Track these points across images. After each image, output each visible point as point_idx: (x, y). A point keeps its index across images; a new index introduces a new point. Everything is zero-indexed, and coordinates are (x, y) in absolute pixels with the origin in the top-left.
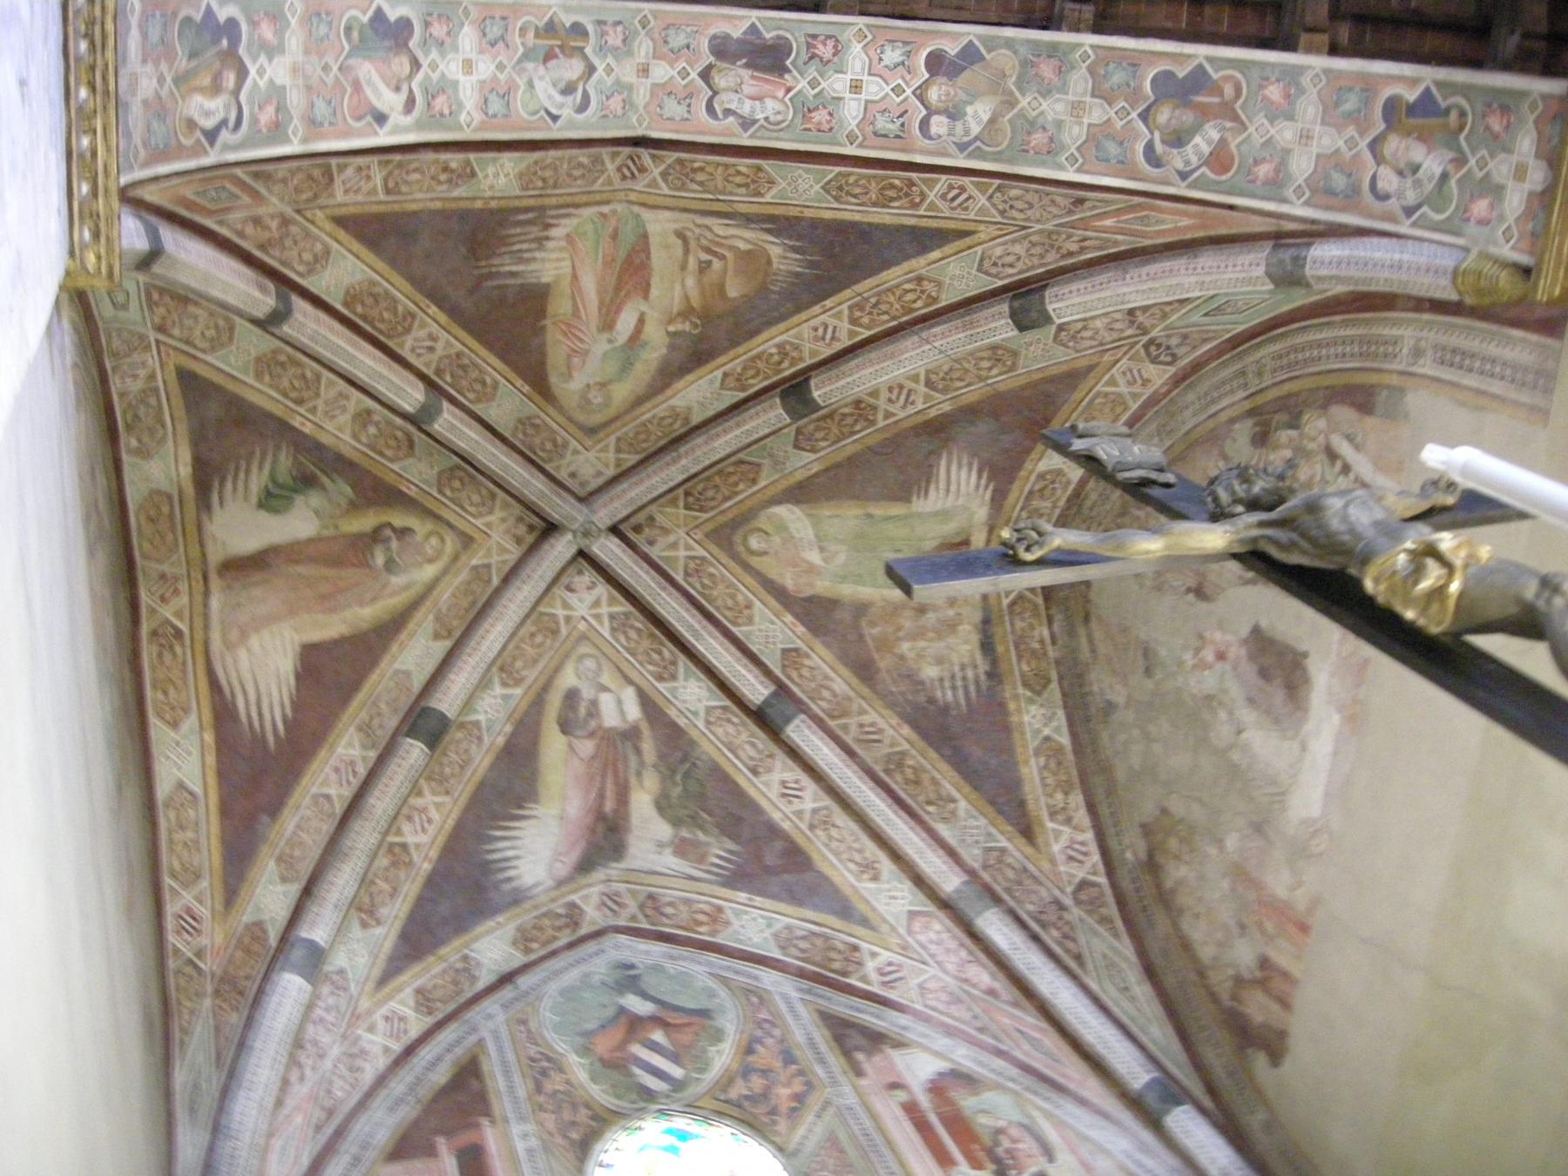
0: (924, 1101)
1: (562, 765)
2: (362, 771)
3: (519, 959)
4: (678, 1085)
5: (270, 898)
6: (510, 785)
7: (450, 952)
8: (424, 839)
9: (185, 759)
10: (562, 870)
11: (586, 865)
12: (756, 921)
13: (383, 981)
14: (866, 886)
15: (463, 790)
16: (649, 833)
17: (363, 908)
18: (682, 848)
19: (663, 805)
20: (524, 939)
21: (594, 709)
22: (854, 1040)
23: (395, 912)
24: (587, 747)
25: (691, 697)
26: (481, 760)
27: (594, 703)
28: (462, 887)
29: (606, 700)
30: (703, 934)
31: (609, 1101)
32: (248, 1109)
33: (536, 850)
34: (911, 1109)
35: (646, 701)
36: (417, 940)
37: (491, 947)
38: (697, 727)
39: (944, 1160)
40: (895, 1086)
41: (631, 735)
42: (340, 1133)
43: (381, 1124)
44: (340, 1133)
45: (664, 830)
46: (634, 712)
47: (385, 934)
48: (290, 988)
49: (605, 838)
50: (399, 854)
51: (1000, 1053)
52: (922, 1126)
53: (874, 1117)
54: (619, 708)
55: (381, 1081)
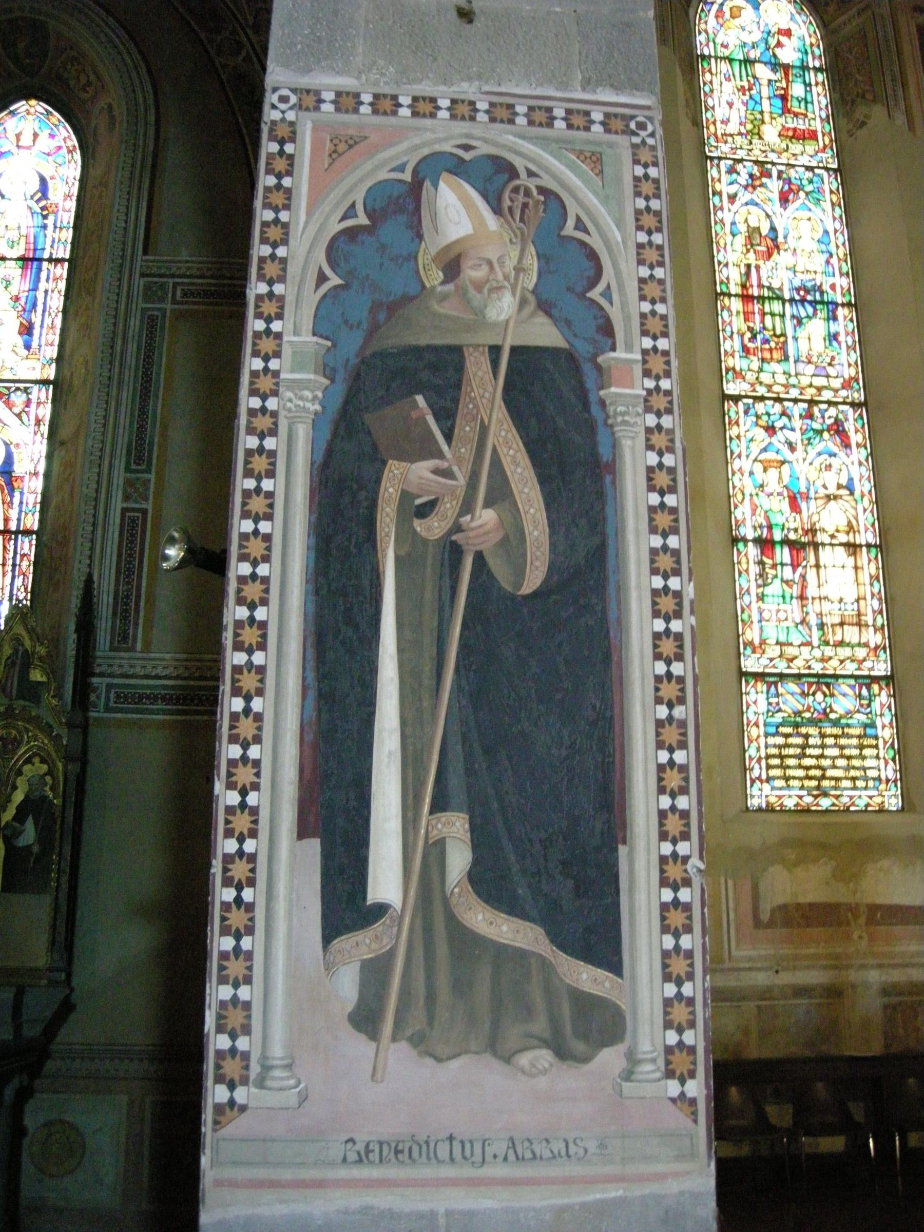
53: (896, 31)
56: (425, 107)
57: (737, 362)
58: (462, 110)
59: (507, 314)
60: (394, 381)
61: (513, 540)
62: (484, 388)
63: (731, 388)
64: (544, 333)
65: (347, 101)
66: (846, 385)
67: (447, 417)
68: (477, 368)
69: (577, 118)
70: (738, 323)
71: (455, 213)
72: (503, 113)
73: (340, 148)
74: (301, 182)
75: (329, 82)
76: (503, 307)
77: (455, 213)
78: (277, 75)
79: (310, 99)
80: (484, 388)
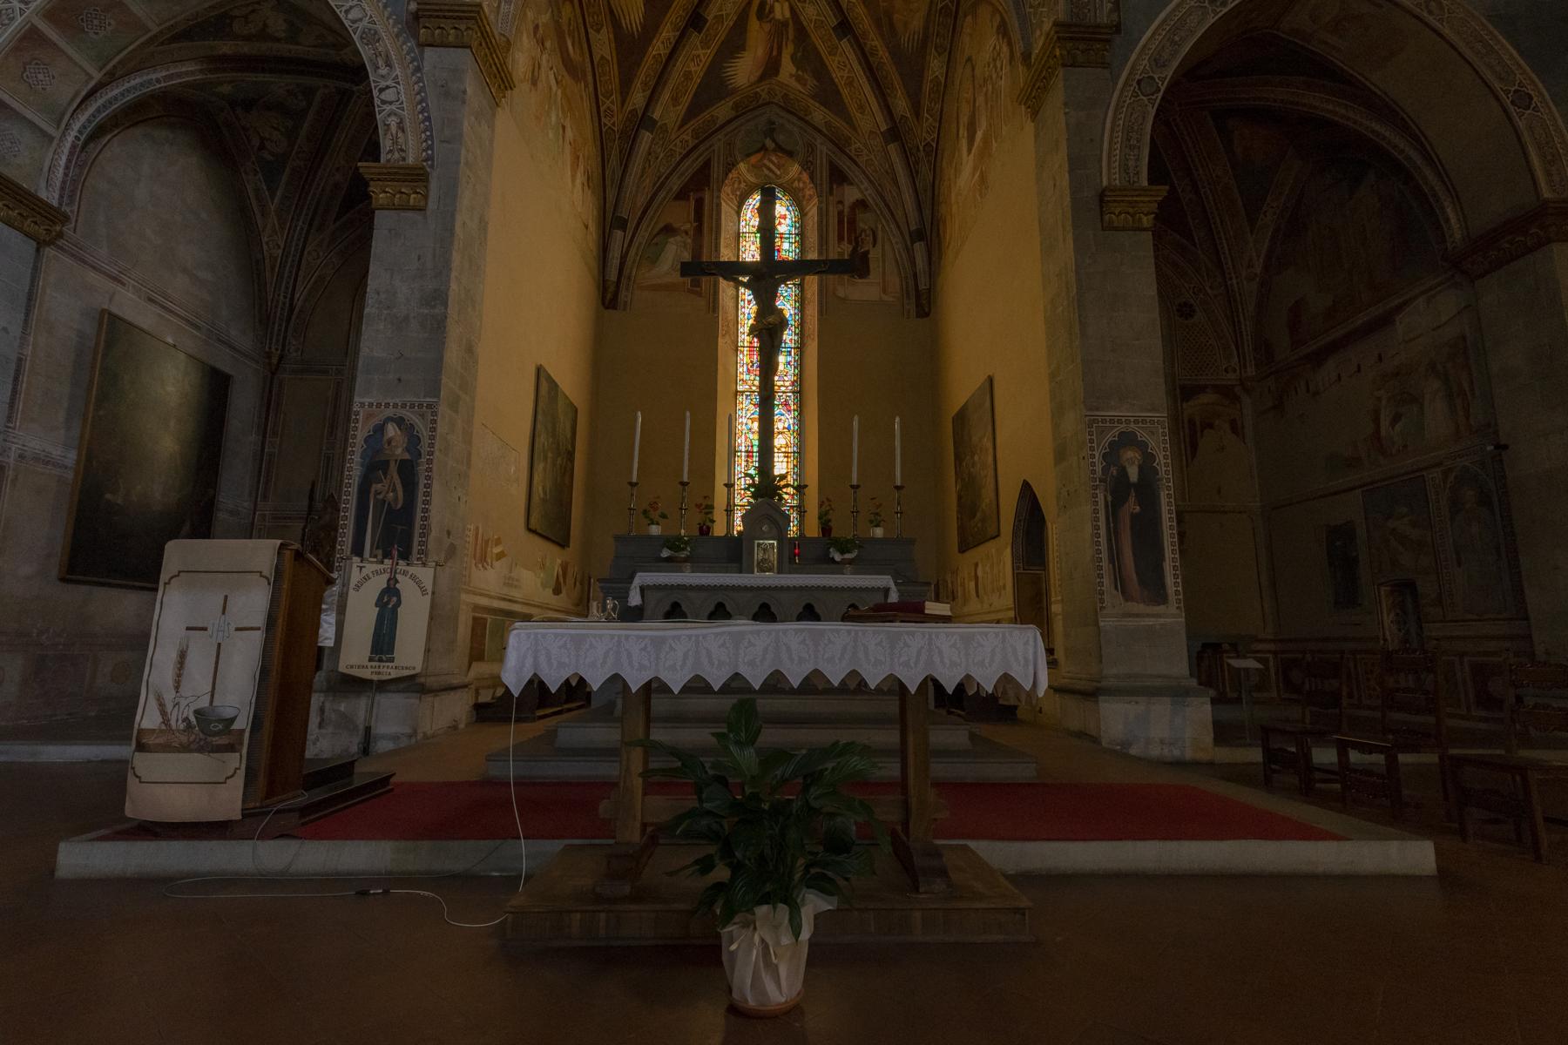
0: (846, 211)
1: (757, 34)
2: (673, 41)
3: (734, 113)
4: (779, 177)
5: (638, 98)
6: (734, 44)
7: (706, 115)
8: (698, 70)
9: (604, 44)
10: (753, 79)
11: (762, 78)
12: (819, 115)
13: (681, 127)
14: (858, 115)
15: (715, 46)
16: (787, 68)
17: (675, 100)
18: (798, 79)
19: (793, 58)
20: (736, 106)
21: (772, 10)
22: (838, 177)
23: (686, 100)
24: (767, 27)
25: (809, 13)
26: (722, 35)
27: (772, 7)
28: (714, 86)
29: (777, 6)
30: (802, 114)
31: (753, 180)
32: (631, 180)
33: (743, 71)
34: (840, 214)
35: (792, 9)
36: (691, 113)
37: (722, 111)
38: (810, 28)
39: (841, 238)
40: (840, 202)
41: (785, 24)
42: (663, 184)
43: (676, 184)
44: (663, 184)
45: (794, 71)
46: (788, 15)
47: (682, 109)
48: (646, 137)
49: (771, 68)
50: (688, 76)
51: (882, 197)
52: (841, 222)
54: (781, 12)
55: (678, 164)
56: (387, 405)
57: (746, 377)
58: (396, 406)
59: (399, 452)
60: (375, 467)
61: (396, 499)
62: (393, 468)
63: (740, 388)
64: (407, 456)
65: (371, 405)
66: (793, 384)
67: (385, 474)
68: (392, 464)
69: (421, 406)
70: (746, 360)
71: (391, 430)
72: (404, 406)
73: (369, 416)
74: (360, 425)
75: (367, 400)
76: (399, 451)
77: (391, 430)
78: (357, 399)
79: (362, 405)
80: (393, 468)
